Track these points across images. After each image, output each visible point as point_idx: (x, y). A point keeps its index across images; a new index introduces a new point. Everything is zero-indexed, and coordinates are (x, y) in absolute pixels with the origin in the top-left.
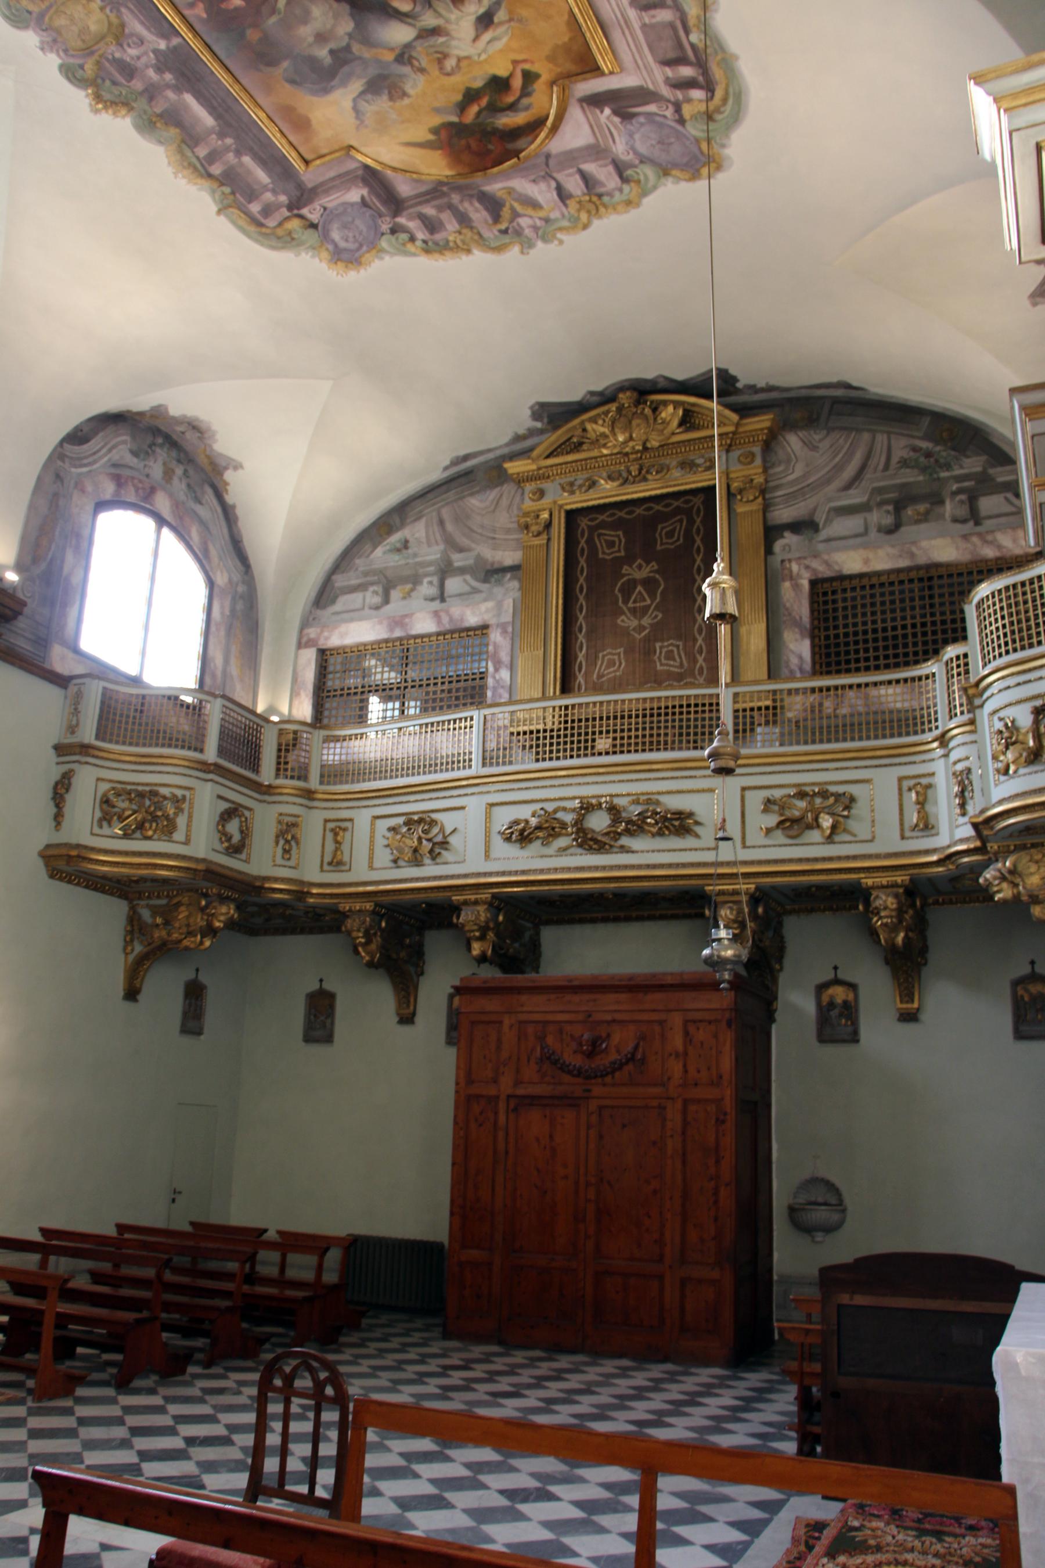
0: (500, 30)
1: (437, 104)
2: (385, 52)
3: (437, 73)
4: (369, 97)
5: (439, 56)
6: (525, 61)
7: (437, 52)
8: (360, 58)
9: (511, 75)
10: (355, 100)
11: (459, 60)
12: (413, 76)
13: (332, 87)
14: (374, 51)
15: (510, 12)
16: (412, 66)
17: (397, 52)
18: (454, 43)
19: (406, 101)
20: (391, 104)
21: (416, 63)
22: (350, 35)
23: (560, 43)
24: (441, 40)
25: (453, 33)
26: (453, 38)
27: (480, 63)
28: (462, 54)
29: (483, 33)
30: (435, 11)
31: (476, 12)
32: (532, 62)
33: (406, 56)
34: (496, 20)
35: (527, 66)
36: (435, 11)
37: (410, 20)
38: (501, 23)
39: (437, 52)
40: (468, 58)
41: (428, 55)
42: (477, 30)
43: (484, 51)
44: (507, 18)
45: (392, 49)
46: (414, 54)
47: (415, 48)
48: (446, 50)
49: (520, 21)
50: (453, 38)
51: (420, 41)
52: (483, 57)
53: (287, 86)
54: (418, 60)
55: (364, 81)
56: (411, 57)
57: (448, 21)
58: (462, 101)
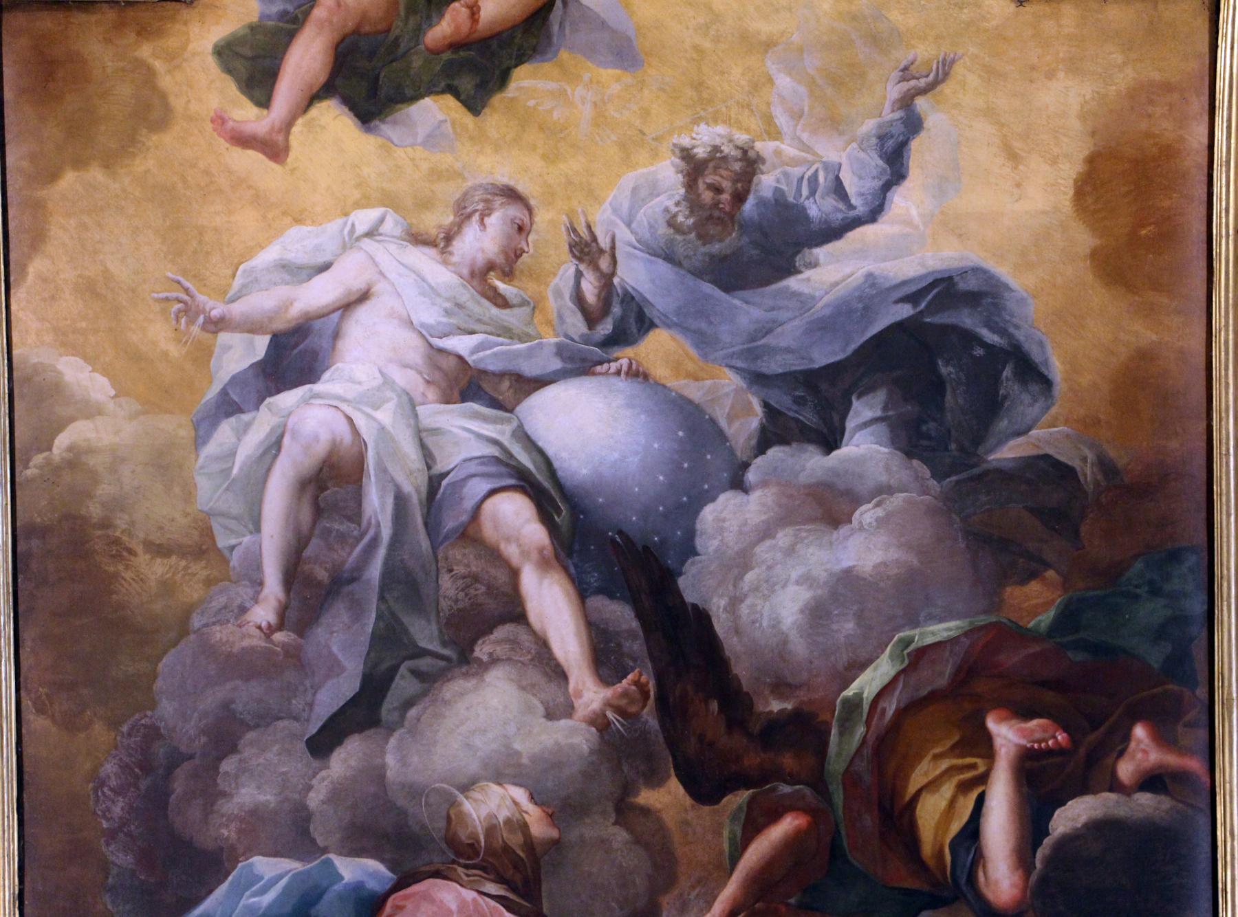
0: (260, 302)
1: (610, 78)
2: (660, 371)
3: (543, 217)
4: (819, 208)
5: (501, 286)
6: (243, 140)
7: (502, 302)
8: (758, 379)
9: (315, 97)
10: (874, 214)
11: (443, 242)
12: (624, 235)
13: (913, 298)
14: (694, 392)
15: (203, 355)
16: (607, 282)
17: (624, 356)
18: (429, 315)
19: (704, 138)
20: (764, 147)
21: (590, 288)
22: (738, 484)
23: (96, 174)
24: (461, 344)
25: (413, 349)
26: (423, 333)
27: (389, 200)
28: (423, 260)
29: (323, 315)
30: (428, 456)
31: (306, 402)
32: (219, 120)
33: (606, 328)
34: (261, 344)
35: (246, 114)
36: (428, 456)
37: (524, 458)
38: (251, 327)
39: (502, 302)
40: (417, 239)
41: (534, 305)
42: (336, 335)
43: (351, 241)
44: (224, 337)
45: (637, 374)
46: (576, 324)
47: (560, 351)
48: (467, 295)
49: (189, 311)
50: (423, 333)
51: (530, 369)
52: (364, 218)
53: (1057, 369)
54: (579, 299)
55: (793, 283)
56: (591, 319)
57: (411, 405)
58: (520, 60)
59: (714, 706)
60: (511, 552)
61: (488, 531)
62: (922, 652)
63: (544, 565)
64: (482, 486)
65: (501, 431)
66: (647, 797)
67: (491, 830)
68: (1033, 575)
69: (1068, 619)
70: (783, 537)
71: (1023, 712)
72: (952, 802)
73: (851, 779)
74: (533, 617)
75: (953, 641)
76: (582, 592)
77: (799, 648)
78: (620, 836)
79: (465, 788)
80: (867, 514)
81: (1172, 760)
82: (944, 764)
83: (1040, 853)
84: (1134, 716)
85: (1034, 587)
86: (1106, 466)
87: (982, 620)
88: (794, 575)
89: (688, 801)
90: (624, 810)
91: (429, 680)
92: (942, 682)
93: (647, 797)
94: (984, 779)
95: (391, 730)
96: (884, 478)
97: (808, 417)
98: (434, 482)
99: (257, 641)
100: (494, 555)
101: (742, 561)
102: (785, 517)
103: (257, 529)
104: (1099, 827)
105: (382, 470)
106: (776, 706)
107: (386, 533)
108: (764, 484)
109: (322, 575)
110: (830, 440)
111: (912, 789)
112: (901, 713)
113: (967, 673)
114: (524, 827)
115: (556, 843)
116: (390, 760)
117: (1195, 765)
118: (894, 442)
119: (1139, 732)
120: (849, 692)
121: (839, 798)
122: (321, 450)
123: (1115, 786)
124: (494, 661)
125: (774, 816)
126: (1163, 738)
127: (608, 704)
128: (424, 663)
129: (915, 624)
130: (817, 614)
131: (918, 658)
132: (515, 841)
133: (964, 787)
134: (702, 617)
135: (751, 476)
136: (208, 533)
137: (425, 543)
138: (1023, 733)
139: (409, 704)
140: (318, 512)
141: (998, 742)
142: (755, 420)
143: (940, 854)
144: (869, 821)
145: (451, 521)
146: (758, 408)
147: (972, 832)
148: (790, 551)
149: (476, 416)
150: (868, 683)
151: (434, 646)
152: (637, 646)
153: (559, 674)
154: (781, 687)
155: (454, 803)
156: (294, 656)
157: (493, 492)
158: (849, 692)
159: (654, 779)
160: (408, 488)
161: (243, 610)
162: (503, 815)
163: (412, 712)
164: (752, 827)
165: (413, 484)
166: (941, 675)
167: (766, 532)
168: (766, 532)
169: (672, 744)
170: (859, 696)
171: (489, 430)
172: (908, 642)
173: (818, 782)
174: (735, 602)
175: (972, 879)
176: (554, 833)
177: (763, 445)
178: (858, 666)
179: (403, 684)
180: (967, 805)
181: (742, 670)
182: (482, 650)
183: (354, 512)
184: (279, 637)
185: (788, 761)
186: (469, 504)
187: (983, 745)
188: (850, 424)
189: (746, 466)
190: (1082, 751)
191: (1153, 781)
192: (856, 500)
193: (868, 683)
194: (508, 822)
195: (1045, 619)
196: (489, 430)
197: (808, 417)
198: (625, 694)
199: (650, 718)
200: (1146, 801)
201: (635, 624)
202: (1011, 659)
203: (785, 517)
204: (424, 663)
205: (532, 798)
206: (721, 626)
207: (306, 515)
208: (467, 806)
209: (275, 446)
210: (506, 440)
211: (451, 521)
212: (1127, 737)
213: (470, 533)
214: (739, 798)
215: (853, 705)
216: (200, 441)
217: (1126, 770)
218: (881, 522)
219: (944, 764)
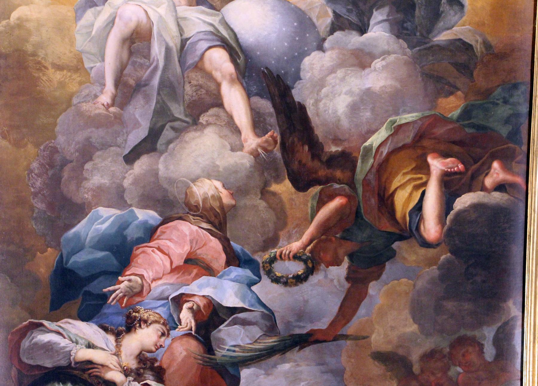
22: (320, 48)
37: (225, 33)
59: (306, 148)
60: (217, 75)
61: (207, 65)
62: (400, 126)
63: (232, 81)
64: (204, 45)
65: (215, 20)
66: (275, 187)
67: (205, 200)
68: (451, 93)
69: (466, 113)
70: (340, 73)
71: (445, 155)
72: (411, 194)
73: (366, 183)
74: (226, 105)
75: (414, 122)
76: (249, 95)
77: (345, 123)
78: (262, 204)
79: (194, 181)
80: (378, 64)
81: (509, 178)
82: (408, 177)
83: (450, 217)
84: (494, 157)
85: (452, 98)
86: (487, 45)
87: (427, 113)
88: (344, 90)
89: (293, 190)
90: (264, 193)
91: (179, 132)
92: (408, 140)
93: (275, 187)
94: (425, 184)
95: (162, 153)
96: (386, 48)
97: (354, 18)
98: (184, 42)
99: (102, 111)
100: (209, 76)
101: (321, 84)
102: (341, 64)
103: (103, 60)
104: (476, 207)
105: (160, 35)
106: (334, 149)
107: (161, 64)
108: (332, 48)
109: (132, 82)
110: (363, 30)
111: (393, 188)
112: (390, 154)
113: (420, 137)
114: (220, 199)
115: (234, 206)
116: (161, 167)
117: (520, 180)
118: (392, 31)
119: (496, 165)
120: (367, 144)
121: (360, 190)
122: (132, 25)
123: (483, 189)
124: (208, 124)
125: (331, 198)
126: (506, 168)
127: (259, 146)
128: (177, 124)
129: (397, 114)
130: (354, 108)
131: (398, 129)
132: (216, 205)
133: (416, 187)
134: (302, 108)
135: (326, 45)
136: (81, 61)
137: (179, 70)
138: (444, 164)
139: (170, 142)
140: (131, 53)
141: (432, 168)
142: (329, 19)
143: (404, 217)
144: (374, 201)
145: (190, 61)
146: (331, 14)
147: (419, 207)
148: (343, 79)
149: (203, 12)
150: (375, 140)
151: (182, 117)
152: (273, 120)
153: (237, 131)
154: (336, 141)
155: (189, 187)
156: (119, 119)
157: (210, 48)
158: (367, 144)
159: (278, 179)
160: (171, 44)
161: (96, 96)
162: (211, 193)
163: (171, 146)
164: (321, 202)
165: (174, 43)
166: (408, 137)
167: (332, 71)
168: (332, 71)
169: (287, 164)
170: (371, 146)
171: (209, 19)
172: (394, 122)
173: (352, 184)
174: (317, 102)
175: (418, 229)
176: (233, 202)
177: (333, 30)
178: (371, 132)
179: (168, 133)
180: (417, 195)
181: (319, 132)
182: (203, 119)
183: (147, 55)
184: (112, 109)
185: (338, 174)
186: (199, 53)
187: (425, 168)
188: (372, 22)
189: (324, 40)
190: (470, 173)
191: (500, 187)
192: (373, 57)
193: (375, 140)
194: (213, 196)
195: (456, 114)
196: (209, 19)
197: (354, 18)
198: (267, 141)
199: (277, 153)
200: (497, 197)
201: (272, 110)
202: (440, 131)
203: (341, 64)
204: (177, 124)
205: (224, 186)
206: (310, 112)
207: (125, 55)
208: (195, 189)
209: (111, 22)
210: (216, 24)
211: (190, 61)
212: (490, 167)
213: (199, 66)
214: (315, 190)
215: (368, 150)
216: (78, 18)
217: (489, 182)
218: (384, 67)
219: (408, 177)
